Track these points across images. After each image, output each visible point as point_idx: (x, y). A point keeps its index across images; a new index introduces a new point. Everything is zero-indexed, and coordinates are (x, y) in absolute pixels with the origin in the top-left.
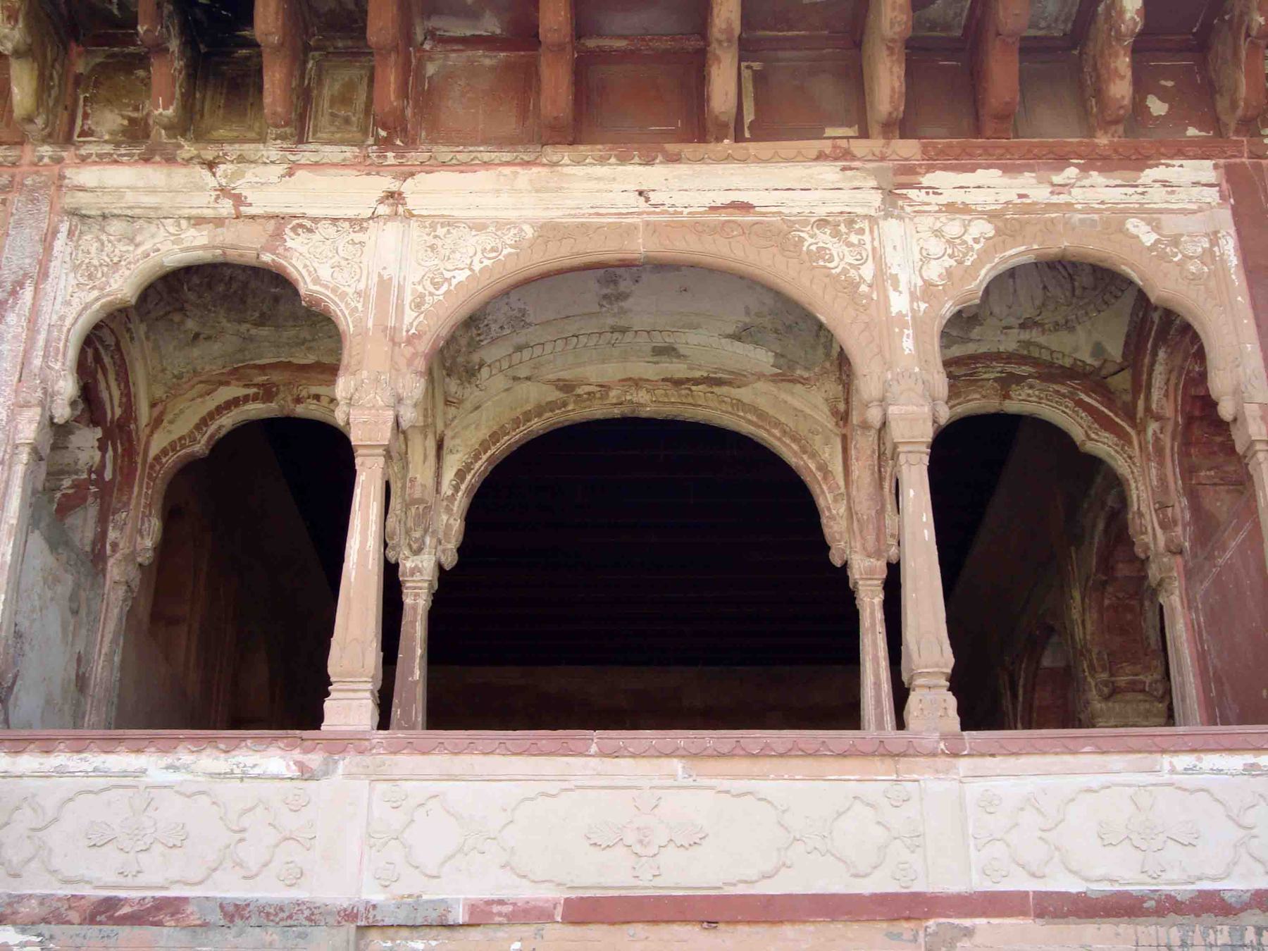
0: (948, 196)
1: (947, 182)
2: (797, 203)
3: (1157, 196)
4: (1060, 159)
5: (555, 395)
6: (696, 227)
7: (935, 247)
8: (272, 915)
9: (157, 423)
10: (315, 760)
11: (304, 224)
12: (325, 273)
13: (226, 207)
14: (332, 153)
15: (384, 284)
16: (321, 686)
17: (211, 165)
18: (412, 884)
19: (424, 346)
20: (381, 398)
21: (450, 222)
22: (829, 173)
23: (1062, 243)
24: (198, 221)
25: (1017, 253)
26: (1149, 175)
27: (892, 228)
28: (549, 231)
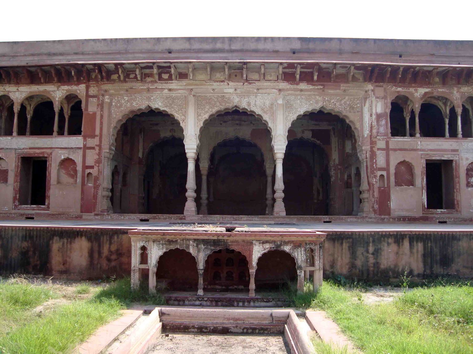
0: (63, 88)
1: (63, 87)
2: (51, 89)
3: (80, 88)
4: (72, 84)
5: (41, 99)
6: (43, 92)
7: (61, 93)
8: (10, 149)
9: (6, 103)
10: (12, 138)
11: (11, 92)
12: (12, 96)
13: (4, 90)
14: (12, 85)
15: (17, 98)
16: (12, 132)
17: (3, 86)
18: (19, 147)
19: (20, 103)
20: (16, 108)
21: (22, 92)
22: (53, 86)
23: (72, 93)
24: (2, 91)
25: (68, 94)
26: (80, 86)
27: (58, 91)
28: (31, 92)
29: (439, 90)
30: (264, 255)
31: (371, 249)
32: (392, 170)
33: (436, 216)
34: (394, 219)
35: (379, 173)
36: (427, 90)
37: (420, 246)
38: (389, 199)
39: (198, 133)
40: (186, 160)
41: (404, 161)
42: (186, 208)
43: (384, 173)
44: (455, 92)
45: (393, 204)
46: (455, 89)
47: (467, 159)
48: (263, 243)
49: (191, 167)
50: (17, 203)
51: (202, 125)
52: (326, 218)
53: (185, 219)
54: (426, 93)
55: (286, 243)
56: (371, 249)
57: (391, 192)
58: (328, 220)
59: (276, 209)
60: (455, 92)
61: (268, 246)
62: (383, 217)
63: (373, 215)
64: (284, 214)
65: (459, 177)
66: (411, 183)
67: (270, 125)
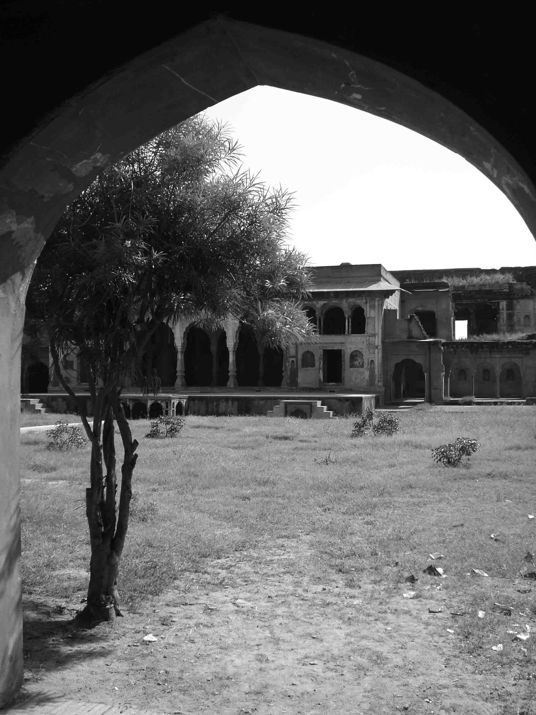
29: (334, 302)
30: (152, 404)
31: (215, 404)
32: (300, 357)
33: (328, 387)
34: (300, 389)
35: (291, 359)
36: (325, 302)
37: (236, 403)
38: (297, 376)
39: (182, 336)
40: (177, 352)
41: (308, 351)
42: (176, 383)
43: (294, 359)
44: (344, 302)
45: (299, 380)
46: (344, 300)
47: (350, 349)
48: (151, 400)
49: (180, 356)
50: (79, 381)
51: (185, 330)
52: (256, 388)
53: (175, 390)
54: (324, 304)
55: (159, 400)
56: (215, 404)
57: (299, 370)
58: (258, 390)
59: (228, 383)
60: (344, 302)
61: (153, 401)
62: (292, 388)
63: (286, 387)
64: (232, 386)
65: (344, 361)
66: (313, 365)
67: (225, 330)
